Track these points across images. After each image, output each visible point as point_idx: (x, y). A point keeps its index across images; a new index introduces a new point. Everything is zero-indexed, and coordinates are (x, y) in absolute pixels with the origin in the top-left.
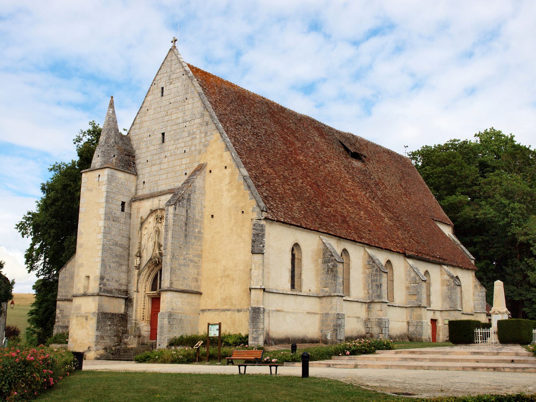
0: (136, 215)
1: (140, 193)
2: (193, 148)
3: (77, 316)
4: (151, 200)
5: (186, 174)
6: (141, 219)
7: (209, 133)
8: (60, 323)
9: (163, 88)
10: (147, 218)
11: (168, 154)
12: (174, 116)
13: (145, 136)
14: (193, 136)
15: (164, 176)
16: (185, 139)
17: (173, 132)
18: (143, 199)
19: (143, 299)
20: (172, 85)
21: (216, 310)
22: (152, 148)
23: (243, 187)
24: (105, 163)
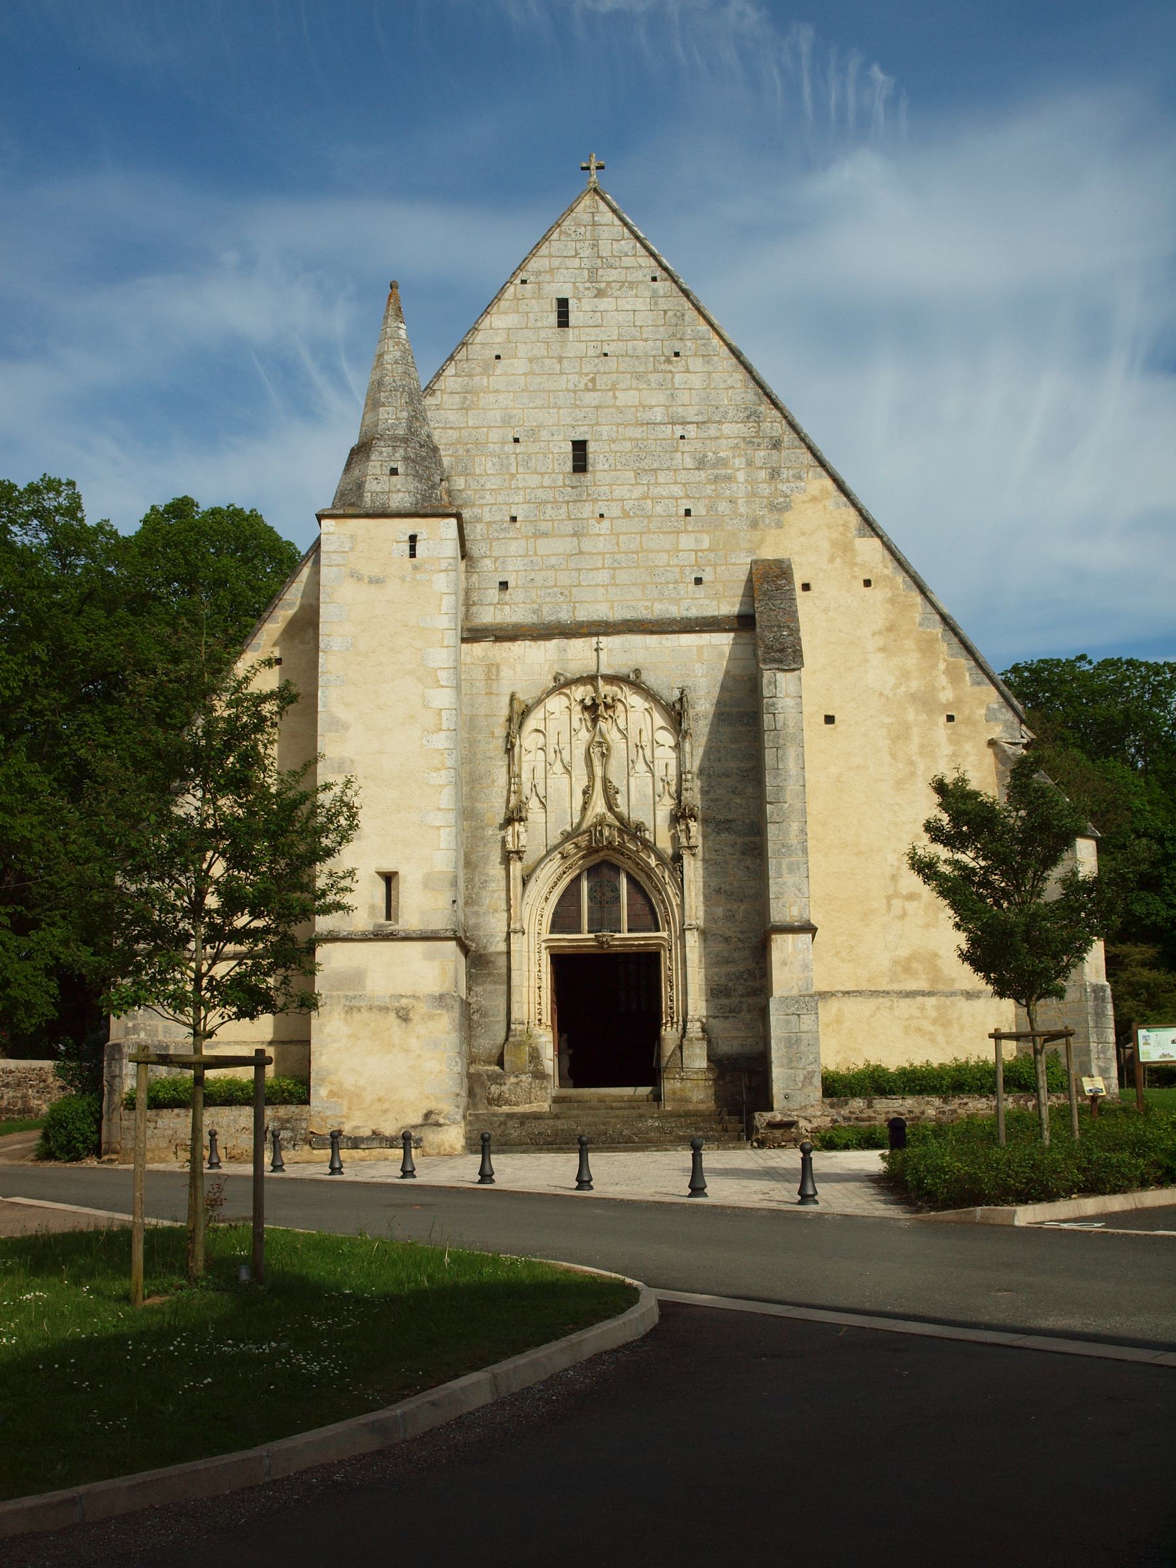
0: (481, 685)
1: (487, 616)
2: (723, 507)
3: (351, 1009)
4: (552, 645)
5: (698, 581)
6: (513, 698)
7: (785, 474)
8: (142, 1035)
9: (563, 304)
10: (540, 701)
11: (614, 511)
12: (623, 398)
13: (495, 435)
14: (722, 472)
15: (603, 577)
16: (683, 476)
17: (628, 446)
18: (513, 638)
19: (534, 957)
20: (605, 303)
21: (874, 994)
22: (533, 481)
23: (943, 647)
24: (425, 498)
